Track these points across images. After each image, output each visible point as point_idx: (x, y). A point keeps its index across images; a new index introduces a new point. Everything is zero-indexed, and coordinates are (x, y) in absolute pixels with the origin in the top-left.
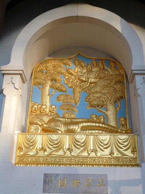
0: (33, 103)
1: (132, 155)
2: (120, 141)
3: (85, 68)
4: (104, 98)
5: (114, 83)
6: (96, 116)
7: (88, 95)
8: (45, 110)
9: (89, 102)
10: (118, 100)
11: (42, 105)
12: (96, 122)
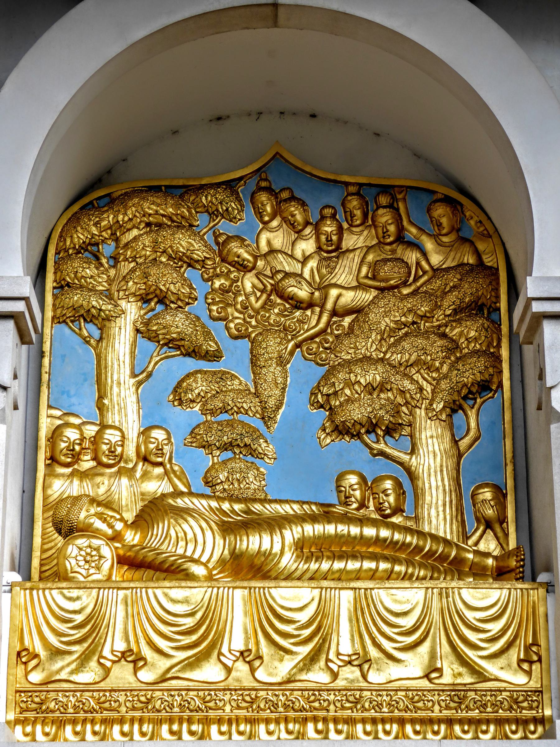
0: (58, 413)
1: (520, 679)
2: (470, 615)
3: (308, 230)
4: (402, 392)
5: (448, 312)
6: (363, 479)
7: (325, 377)
8: (119, 450)
9: (331, 409)
10: (465, 398)
11: (104, 427)
12: (362, 521)
